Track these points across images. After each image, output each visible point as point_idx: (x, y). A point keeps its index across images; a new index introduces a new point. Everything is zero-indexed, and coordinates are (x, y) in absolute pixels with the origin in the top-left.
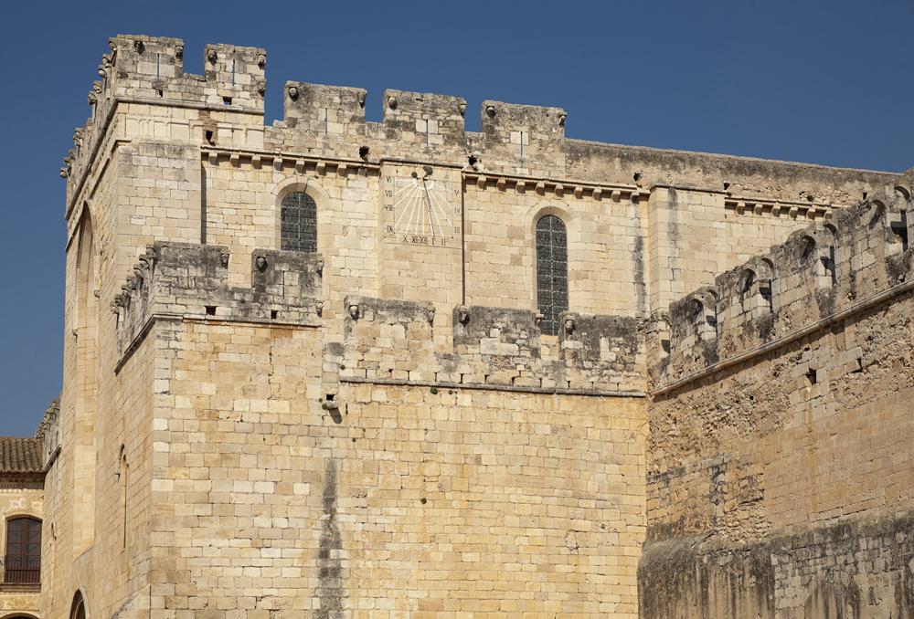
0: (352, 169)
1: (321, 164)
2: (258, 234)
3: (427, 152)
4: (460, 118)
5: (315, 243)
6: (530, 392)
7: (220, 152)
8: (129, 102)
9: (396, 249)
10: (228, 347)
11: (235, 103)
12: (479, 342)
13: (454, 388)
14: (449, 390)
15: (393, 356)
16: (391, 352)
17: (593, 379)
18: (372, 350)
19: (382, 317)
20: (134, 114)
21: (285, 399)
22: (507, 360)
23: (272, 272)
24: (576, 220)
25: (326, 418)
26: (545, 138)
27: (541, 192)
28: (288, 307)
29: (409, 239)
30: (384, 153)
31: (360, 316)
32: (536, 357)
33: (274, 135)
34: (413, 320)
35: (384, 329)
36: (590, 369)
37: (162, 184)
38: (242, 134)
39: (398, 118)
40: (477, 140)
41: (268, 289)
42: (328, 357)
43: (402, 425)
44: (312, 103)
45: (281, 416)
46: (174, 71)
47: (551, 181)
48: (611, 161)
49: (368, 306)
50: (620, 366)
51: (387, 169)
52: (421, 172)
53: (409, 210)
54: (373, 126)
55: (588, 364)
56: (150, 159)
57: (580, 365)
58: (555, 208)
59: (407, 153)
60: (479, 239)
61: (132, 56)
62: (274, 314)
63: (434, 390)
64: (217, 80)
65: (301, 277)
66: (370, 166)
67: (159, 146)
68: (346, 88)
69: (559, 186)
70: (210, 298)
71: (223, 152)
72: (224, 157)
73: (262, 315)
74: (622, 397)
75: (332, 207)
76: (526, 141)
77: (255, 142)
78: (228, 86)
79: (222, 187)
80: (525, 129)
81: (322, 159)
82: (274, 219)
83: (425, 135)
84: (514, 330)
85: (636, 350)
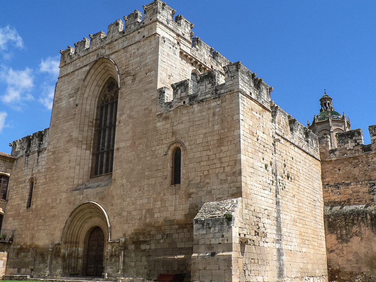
78: (184, 30)
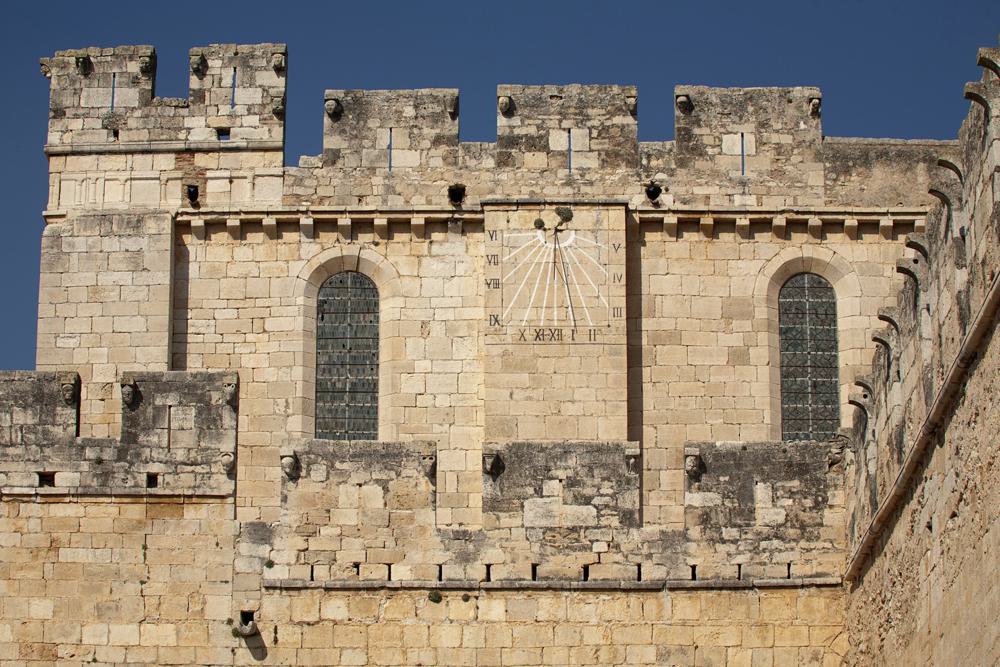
0: (433, 225)
1: (380, 221)
2: (273, 347)
3: (569, 182)
4: (630, 120)
5: (376, 355)
6: (615, 590)
7: (209, 217)
8: (66, 154)
9: (505, 354)
10: (75, 538)
11: (236, 136)
12: (522, 506)
13: (471, 589)
14: (462, 593)
15: (361, 540)
16: (358, 531)
17: (740, 559)
18: (324, 531)
19: (342, 473)
20: (73, 172)
21: (168, 622)
22: (575, 535)
23: (150, 410)
24: (851, 279)
25: (239, 652)
26: (786, 139)
27: (784, 233)
28: (175, 466)
29: (530, 335)
30: (492, 192)
31: (303, 473)
32: (631, 525)
33: (299, 182)
34: (398, 475)
35: (346, 493)
36: (735, 542)
37: (106, 279)
38: (246, 184)
39: (517, 132)
40: (660, 155)
41: (142, 438)
42: (245, 547)
43: (374, 659)
44: (366, 122)
45: (162, 651)
46: (137, 96)
47: (797, 213)
48: (910, 168)
49: (318, 455)
50: (792, 532)
51: (493, 219)
52: (551, 218)
53: (530, 284)
54: (473, 149)
55: (729, 533)
56: (90, 240)
57: (716, 535)
58: (812, 259)
59: (534, 189)
60: (668, 325)
61: (73, 82)
62: (152, 480)
63: (436, 596)
64: (207, 102)
65: (199, 413)
66: (466, 216)
67: (105, 217)
68: (425, 91)
69: (814, 221)
70: (45, 458)
71: (214, 217)
72: (214, 225)
73: (131, 483)
74: (795, 587)
75: (403, 291)
76: (750, 147)
77: (269, 197)
78: (225, 109)
79: (215, 273)
80: (749, 128)
81: (381, 212)
82: (301, 319)
83: (566, 155)
84: (589, 482)
85: (825, 500)
